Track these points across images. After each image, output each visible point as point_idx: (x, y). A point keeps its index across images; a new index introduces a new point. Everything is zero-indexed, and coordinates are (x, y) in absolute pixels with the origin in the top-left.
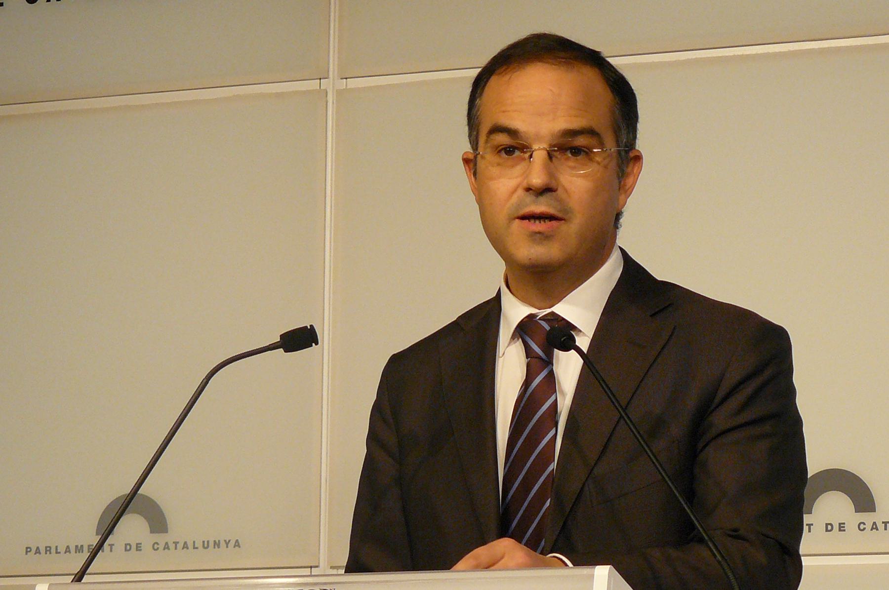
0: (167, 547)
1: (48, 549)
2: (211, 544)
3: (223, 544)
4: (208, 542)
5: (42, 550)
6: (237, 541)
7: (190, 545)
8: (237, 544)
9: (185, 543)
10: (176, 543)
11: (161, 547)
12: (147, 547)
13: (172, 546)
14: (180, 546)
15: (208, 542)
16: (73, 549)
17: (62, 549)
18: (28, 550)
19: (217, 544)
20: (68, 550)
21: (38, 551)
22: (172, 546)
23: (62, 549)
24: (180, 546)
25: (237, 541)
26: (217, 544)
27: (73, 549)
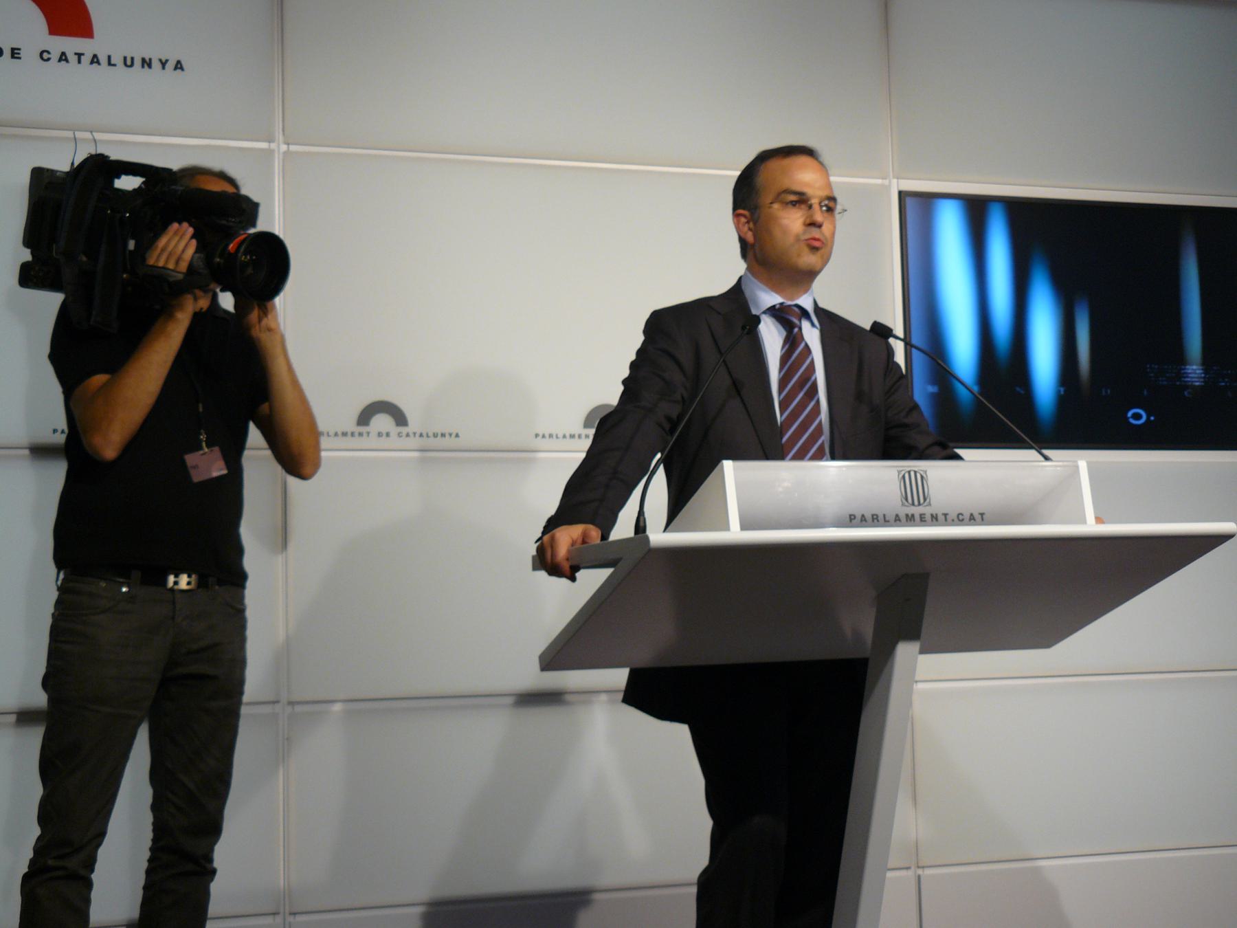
0: (63, 57)
3: (156, 64)
4: (132, 59)
6: (179, 62)
7: (103, 60)
8: (179, 66)
9: (95, 56)
10: (79, 55)
11: (55, 56)
13: (72, 58)
14: (86, 59)
15: (132, 59)
19: (147, 63)
22: (72, 58)
24: (86, 59)
25: (179, 62)
26: (147, 63)
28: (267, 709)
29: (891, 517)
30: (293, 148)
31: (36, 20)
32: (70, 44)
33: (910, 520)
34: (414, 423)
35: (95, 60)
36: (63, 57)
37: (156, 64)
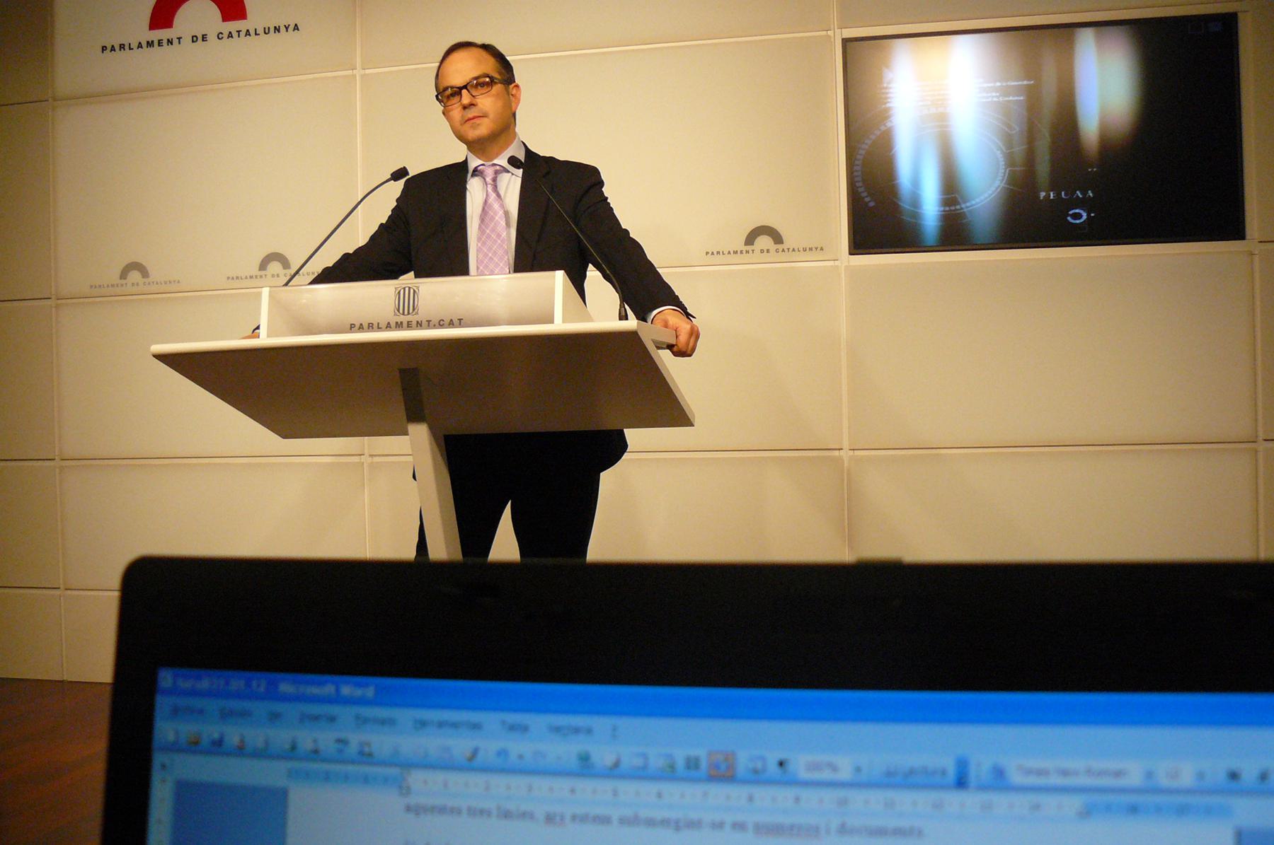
0: (230, 35)
1: (122, 47)
2: (272, 30)
5: (117, 48)
7: (252, 32)
8: (296, 28)
11: (226, 35)
12: (212, 37)
14: (243, 34)
16: (144, 44)
17: (134, 45)
18: (104, 48)
19: (277, 29)
20: (140, 46)
21: (113, 49)
23: (134, 45)
24: (243, 34)
26: (277, 29)
27: (144, 44)
28: (356, 459)
29: (383, 325)
30: (368, 71)
31: (215, 12)
32: (233, 26)
33: (399, 326)
34: (789, 241)
35: (248, 33)
36: (230, 35)
37: (283, 29)
